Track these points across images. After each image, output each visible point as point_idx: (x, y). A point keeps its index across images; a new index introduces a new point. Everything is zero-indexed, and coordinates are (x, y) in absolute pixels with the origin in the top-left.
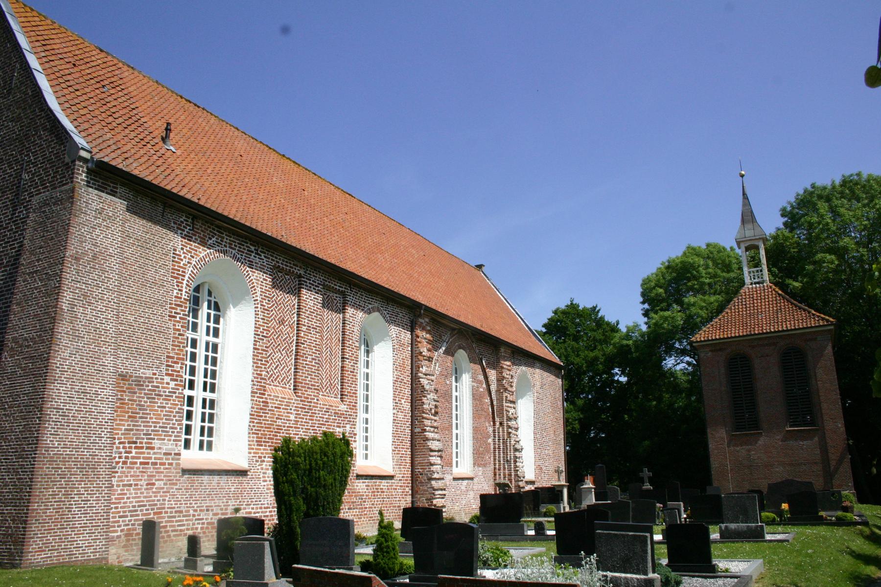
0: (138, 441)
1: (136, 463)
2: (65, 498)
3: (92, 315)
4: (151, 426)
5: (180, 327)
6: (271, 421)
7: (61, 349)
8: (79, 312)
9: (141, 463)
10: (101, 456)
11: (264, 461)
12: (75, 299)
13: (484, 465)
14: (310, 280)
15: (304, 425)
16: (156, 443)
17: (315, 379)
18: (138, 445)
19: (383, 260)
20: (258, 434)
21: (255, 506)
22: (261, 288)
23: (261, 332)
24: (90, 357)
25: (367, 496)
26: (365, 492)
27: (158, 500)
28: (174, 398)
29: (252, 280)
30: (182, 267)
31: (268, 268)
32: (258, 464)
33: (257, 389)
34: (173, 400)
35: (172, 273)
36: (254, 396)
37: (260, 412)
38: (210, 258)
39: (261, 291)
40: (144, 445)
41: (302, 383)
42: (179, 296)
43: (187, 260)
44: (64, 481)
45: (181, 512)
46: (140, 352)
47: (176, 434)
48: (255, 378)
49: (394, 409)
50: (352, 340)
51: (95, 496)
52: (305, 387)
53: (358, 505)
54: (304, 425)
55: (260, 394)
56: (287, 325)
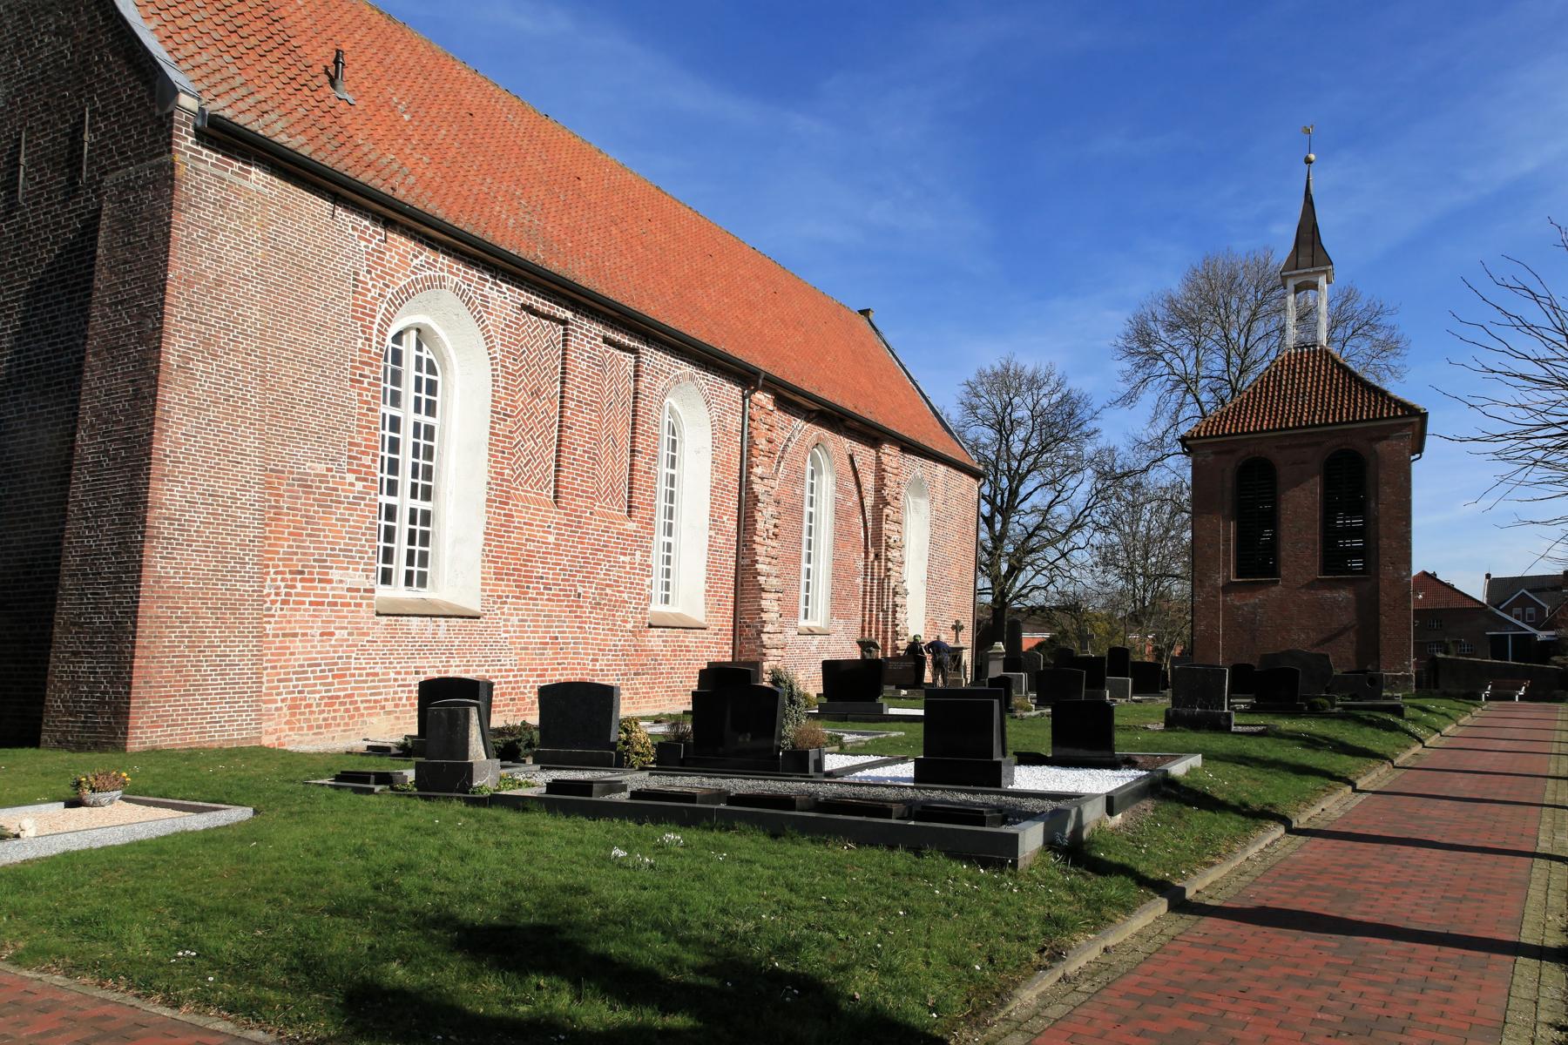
0: (306, 570)
1: (303, 603)
2: (189, 652)
3: (220, 376)
4: (326, 549)
5: (369, 399)
6: (518, 544)
7: (171, 427)
8: (197, 370)
9: (311, 603)
10: (244, 591)
11: (505, 603)
12: (189, 349)
13: (847, 617)
14: (582, 328)
15: (570, 551)
16: (335, 574)
17: (588, 482)
18: (306, 576)
19: (706, 299)
20: (497, 562)
21: (491, 668)
22: (501, 339)
23: (502, 408)
24: (221, 441)
25: (663, 655)
26: (662, 651)
27: (339, 658)
28: (362, 506)
29: (487, 326)
30: (370, 303)
31: (513, 307)
32: (496, 606)
33: (495, 495)
34: (362, 510)
35: (353, 311)
36: (491, 507)
37: (500, 531)
38: (415, 288)
39: (502, 345)
40: (316, 576)
41: (567, 488)
42: (367, 348)
43: (378, 291)
44: (187, 627)
45: (376, 674)
46: (305, 435)
47: (366, 560)
48: (492, 478)
49: (711, 529)
50: (648, 423)
51: (237, 649)
52: (571, 494)
53: (650, 669)
54: (570, 551)
55: (500, 502)
56: (544, 399)
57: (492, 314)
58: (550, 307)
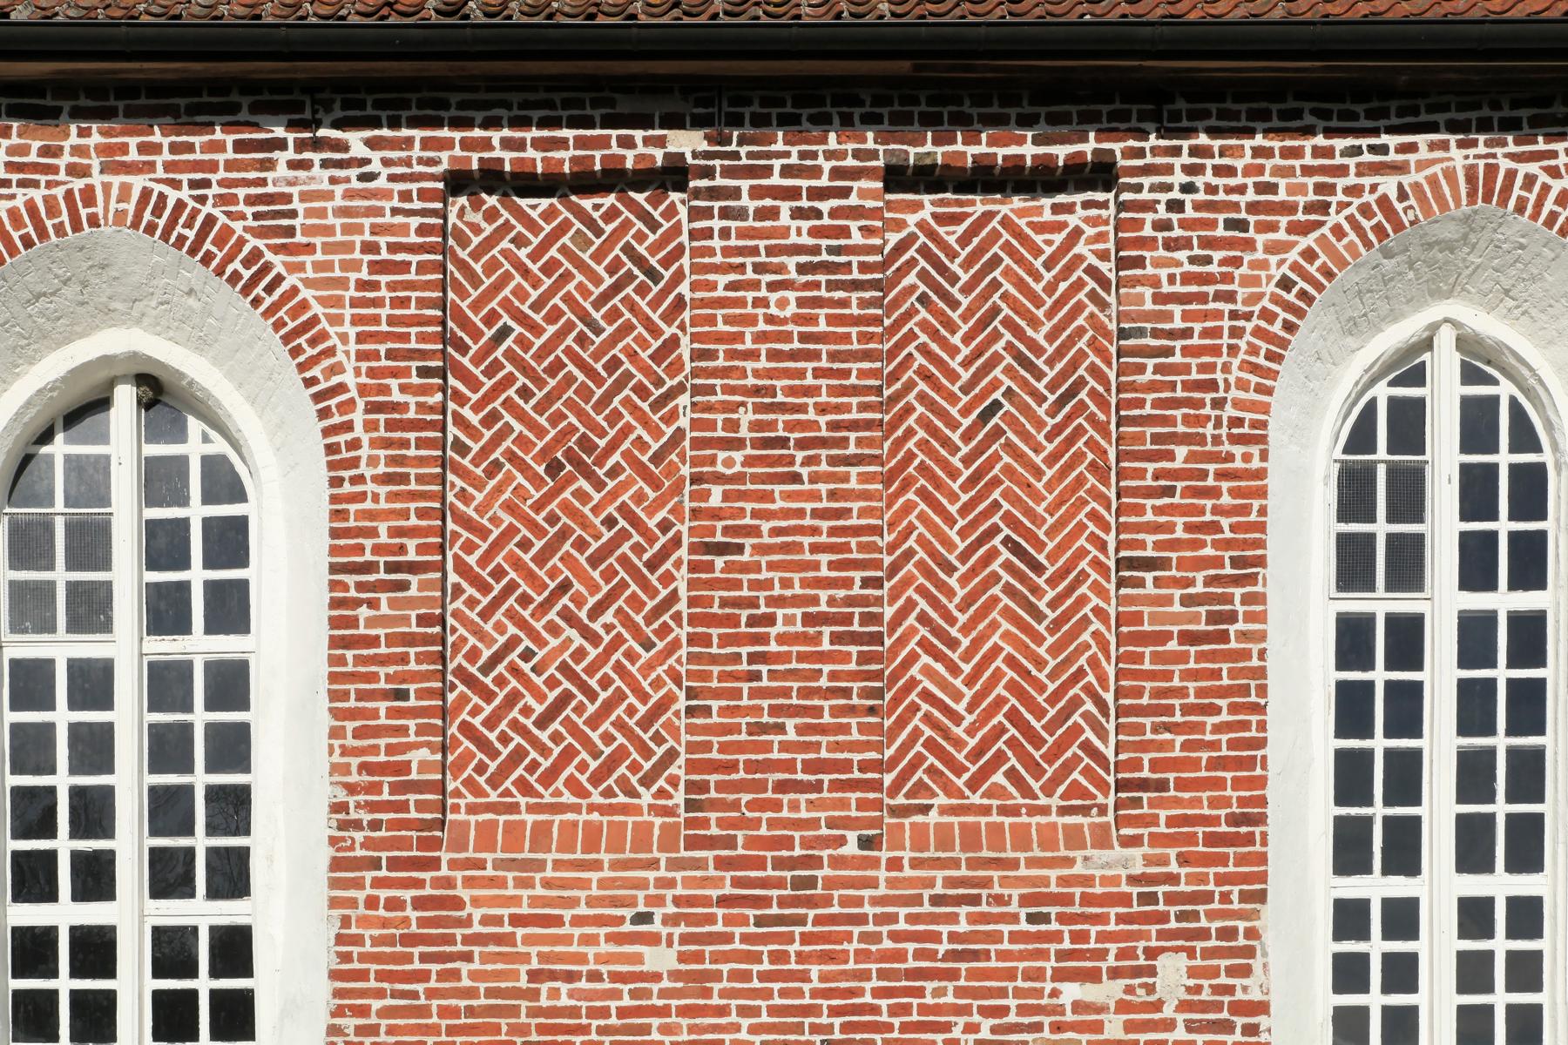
48: (352, 789)
57: (309, 248)
58: (581, 143)
